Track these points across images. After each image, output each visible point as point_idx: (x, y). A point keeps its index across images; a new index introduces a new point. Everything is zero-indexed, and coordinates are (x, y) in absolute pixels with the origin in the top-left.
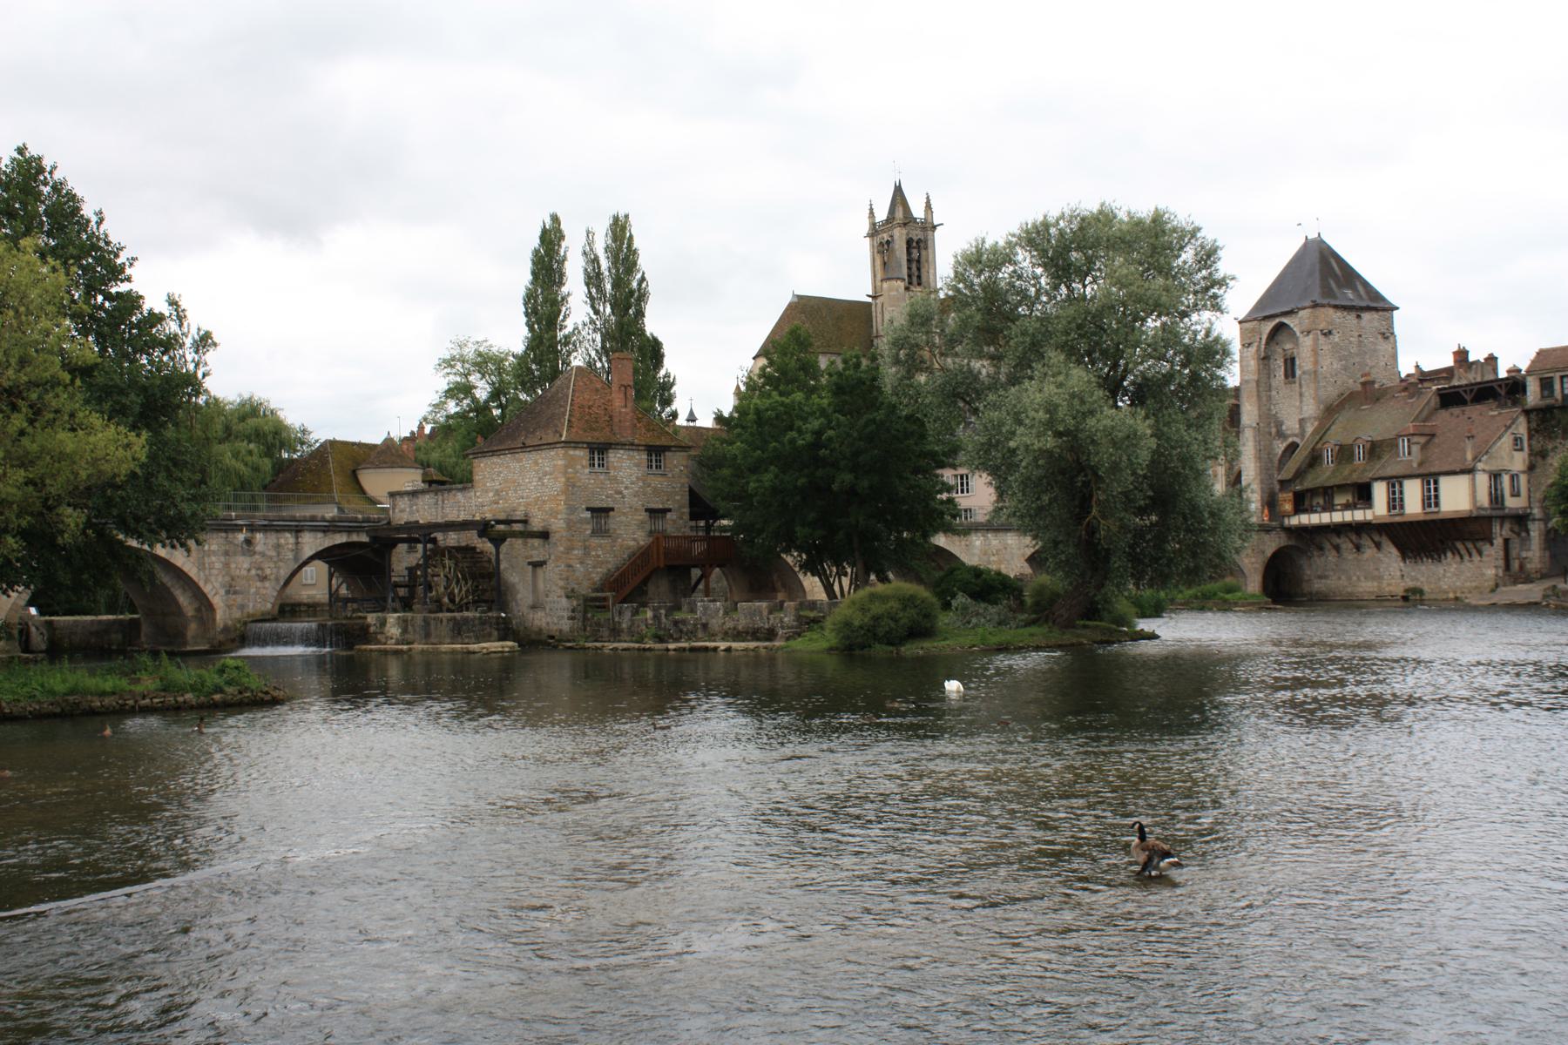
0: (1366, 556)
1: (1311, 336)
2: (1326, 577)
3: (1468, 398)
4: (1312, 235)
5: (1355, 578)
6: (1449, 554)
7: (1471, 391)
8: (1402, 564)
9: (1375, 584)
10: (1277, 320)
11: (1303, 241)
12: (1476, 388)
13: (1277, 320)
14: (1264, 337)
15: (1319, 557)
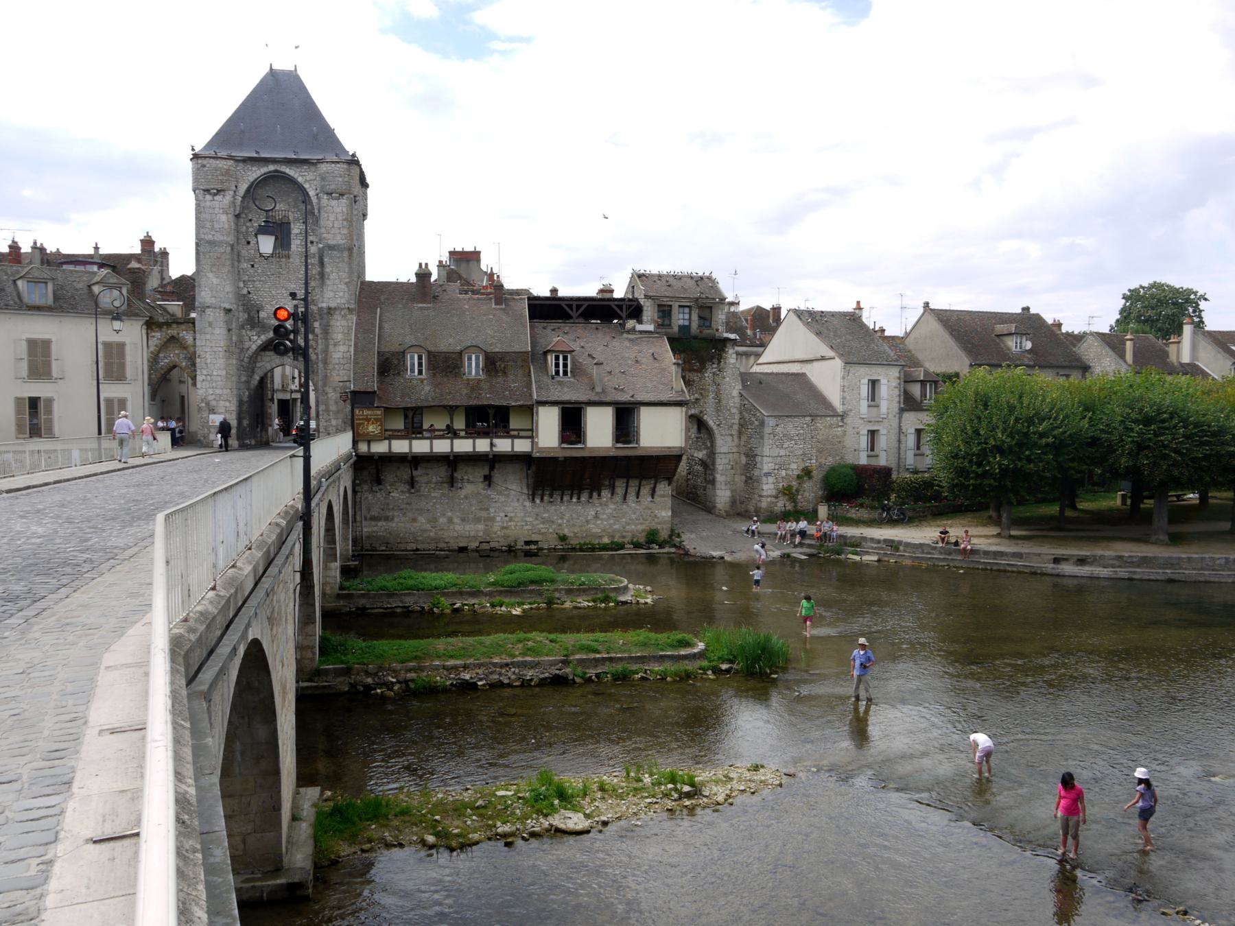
0: (463, 493)
1: (344, 201)
2: (387, 519)
3: (574, 314)
4: (283, 64)
5: (442, 520)
6: (606, 493)
7: (578, 307)
8: (527, 504)
9: (481, 527)
10: (272, 167)
11: (267, 69)
12: (586, 304)
13: (272, 167)
14: (243, 187)
15: (372, 491)
